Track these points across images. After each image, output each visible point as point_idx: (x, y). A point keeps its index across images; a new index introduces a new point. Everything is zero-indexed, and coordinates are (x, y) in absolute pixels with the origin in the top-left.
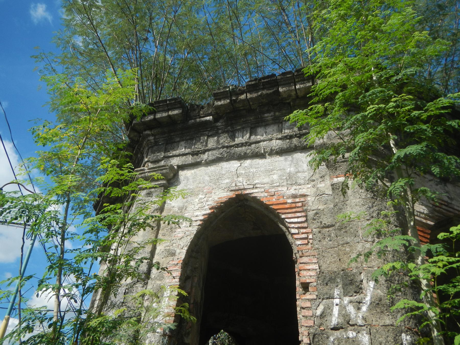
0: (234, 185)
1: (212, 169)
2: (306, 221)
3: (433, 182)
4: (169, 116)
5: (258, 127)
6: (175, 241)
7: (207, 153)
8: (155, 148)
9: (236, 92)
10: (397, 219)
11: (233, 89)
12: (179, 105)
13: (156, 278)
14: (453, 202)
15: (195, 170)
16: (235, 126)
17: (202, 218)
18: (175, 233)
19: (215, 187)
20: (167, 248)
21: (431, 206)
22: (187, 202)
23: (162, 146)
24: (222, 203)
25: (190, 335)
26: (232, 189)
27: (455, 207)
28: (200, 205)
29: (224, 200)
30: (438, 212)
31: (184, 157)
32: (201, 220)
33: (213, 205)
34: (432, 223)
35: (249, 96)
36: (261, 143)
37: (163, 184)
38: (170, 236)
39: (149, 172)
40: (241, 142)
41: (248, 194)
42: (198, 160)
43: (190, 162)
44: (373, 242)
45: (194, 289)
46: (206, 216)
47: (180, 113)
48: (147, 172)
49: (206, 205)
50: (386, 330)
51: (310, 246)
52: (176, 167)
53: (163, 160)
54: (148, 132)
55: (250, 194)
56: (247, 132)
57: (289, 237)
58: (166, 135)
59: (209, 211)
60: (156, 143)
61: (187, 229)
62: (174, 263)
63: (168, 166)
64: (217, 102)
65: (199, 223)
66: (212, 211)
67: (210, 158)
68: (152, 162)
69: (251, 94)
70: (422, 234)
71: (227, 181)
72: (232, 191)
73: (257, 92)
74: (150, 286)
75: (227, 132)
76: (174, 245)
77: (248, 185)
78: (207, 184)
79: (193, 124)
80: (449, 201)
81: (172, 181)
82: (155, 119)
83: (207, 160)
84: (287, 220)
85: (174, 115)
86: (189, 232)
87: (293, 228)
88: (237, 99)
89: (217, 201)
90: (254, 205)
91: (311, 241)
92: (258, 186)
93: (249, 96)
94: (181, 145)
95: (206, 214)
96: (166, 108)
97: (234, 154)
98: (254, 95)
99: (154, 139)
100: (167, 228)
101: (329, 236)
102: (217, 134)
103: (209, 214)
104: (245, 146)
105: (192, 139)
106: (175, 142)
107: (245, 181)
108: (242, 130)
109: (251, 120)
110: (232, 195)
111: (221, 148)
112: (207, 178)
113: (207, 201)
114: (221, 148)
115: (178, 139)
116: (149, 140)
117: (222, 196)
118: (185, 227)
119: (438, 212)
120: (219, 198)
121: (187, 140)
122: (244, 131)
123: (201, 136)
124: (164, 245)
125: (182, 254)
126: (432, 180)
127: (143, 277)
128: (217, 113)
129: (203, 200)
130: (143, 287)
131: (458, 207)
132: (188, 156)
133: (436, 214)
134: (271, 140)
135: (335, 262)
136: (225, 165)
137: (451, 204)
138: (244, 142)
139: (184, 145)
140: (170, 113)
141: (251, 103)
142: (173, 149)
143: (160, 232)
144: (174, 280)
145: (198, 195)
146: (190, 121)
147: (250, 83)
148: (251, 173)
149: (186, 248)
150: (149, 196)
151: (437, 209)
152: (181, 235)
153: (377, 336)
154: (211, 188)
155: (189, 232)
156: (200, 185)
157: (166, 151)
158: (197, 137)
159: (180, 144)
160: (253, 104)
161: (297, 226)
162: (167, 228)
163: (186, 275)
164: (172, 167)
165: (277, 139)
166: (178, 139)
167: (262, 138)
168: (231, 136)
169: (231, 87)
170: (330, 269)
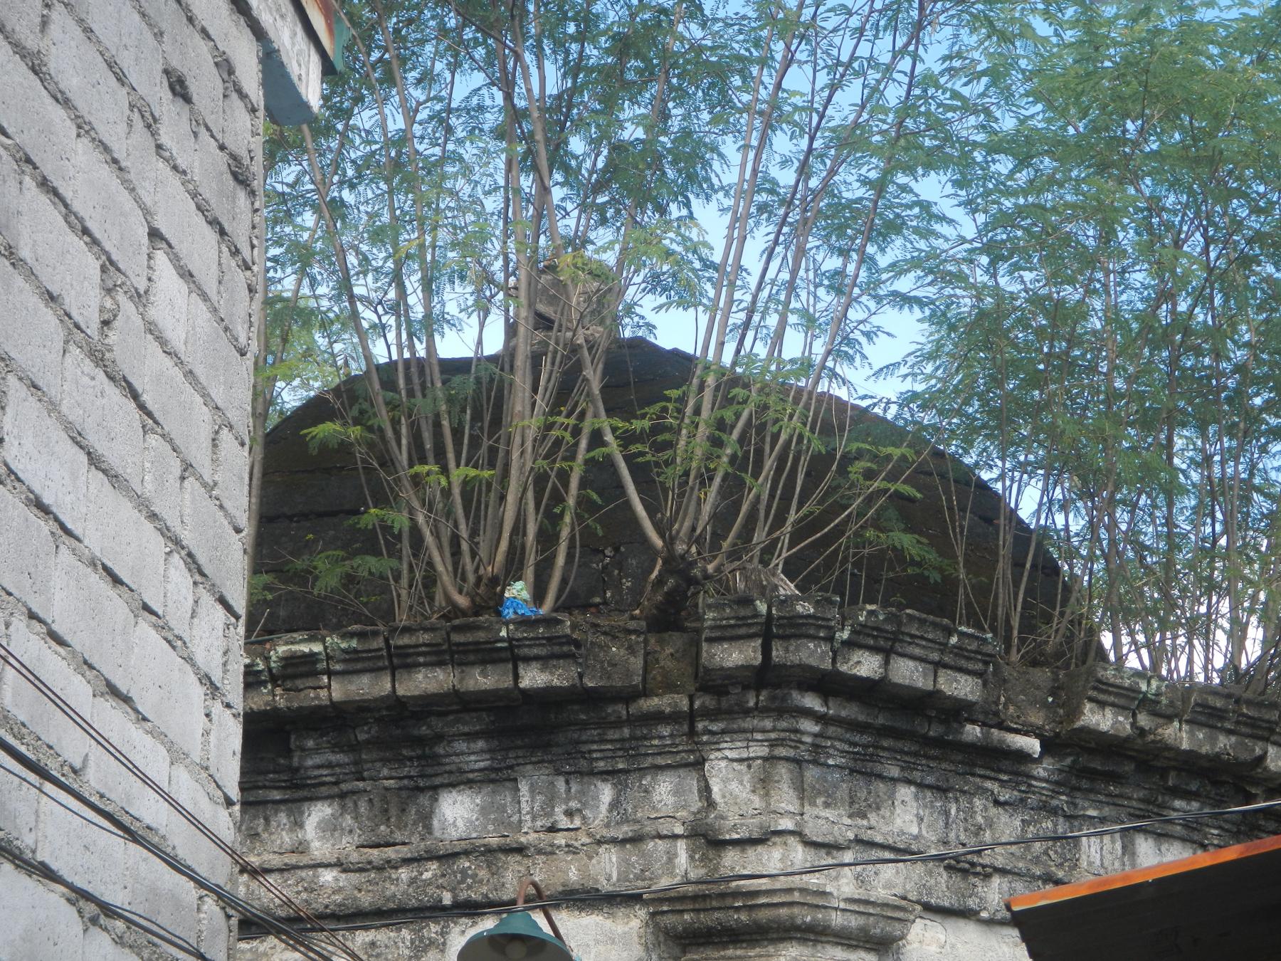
7: (996, 880)
16: (1080, 802)
42: (972, 903)
43: (947, 904)
54: (811, 702)
58: (866, 739)
68: (810, 844)
96: (935, 656)
105: (941, 790)
106: (880, 777)
114: (1039, 878)
115: (895, 772)
116: (796, 731)
121: (921, 786)
123: (974, 795)
139: (913, 807)
146: (969, 727)
166: (895, 772)
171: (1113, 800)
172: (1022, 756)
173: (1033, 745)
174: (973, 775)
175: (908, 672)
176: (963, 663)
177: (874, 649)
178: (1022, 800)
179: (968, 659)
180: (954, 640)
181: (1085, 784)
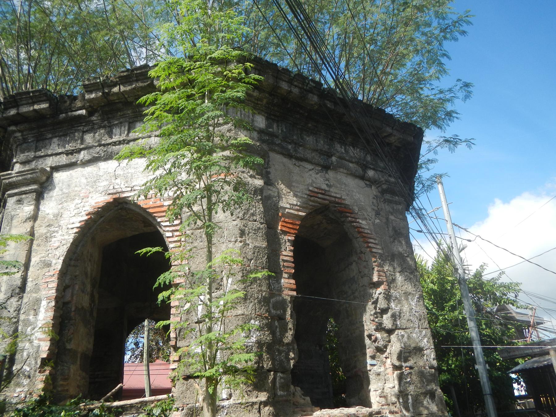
0: (111, 187)
1: (90, 170)
2: (181, 222)
3: (313, 171)
4: (35, 110)
5: (137, 121)
6: (50, 251)
7: (82, 152)
8: (24, 146)
9: (108, 84)
10: (264, 216)
11: (104, 80)
12: (45, 98)
13: (31, 291)
14: (331, 190)
15: (71, 172)
16: (112, 121)
17: (79, 225)
18: (51, 243)
19: (92, 190)
20: (42, 259)
21: (306, 196)
22: (62, 208)
23: (32, 144)
24: (99, 208)
25: (73, 341)
26: (110, 192)
27: (333, 194)
28: (77, 210)
29: (101, 205)
30: (313, 201)
31: (58, 156)
32: (77, 228)
33: (90, 211)
34: (304, 214)
35: (123, 88)
36: (140, 141)
37: (35, 189)
38: (45, 246)
39: (17, 176)
40: (119, 139)
41: (125, 197)
42: (73, 161)
43: (65, 163)
44: (236, 242)
45: (75, 296)
46: (83, 223)
47: (47, 108)
48: (14, 177)
49: (83, 211)
50: (237, 319)
51: (181, 249)
52: (48, 169)
53: (34, 160)
54: (13, 128)
55: (128, 197)
56: (125, 127)
57: (166, 239)
59: (86, 218)
60: (25, 141)
61: (63, 238)
62: (50, 274)
63: (38, 169)
64: (88, 94)
65: (76, 230)
66: (89, 217)
67: (88, 157)
69: (124, 87)
70: (291, 226)
71: (105, 183)
72: (109, 194)
73: (132, 85)
74: (25, 300)
75: (104, 127)
76: (50, 255)
77: (126, 187)
78: (84, 187)
79: (64, 118)
80: (327, 189)
81: (46, 185)
82: (18, 114)
83: (83, 161)
84: (162, 223)
85: (40, 109)
86: (65, 241)
87: (168, 231)
88: (110, 91)
89: (94, 206)
90: (133, 208)
91: (183, 243)
92: (135, 188)
93: (123, 88)
94: (54, 142)
95: (83, 221)
96: (30, 101)
97: (111, 152)
98: (128, 88)
99: (22, 135)
100: (42, 238)
101: (201, 237)
102: (92, 130)
103: (86, 221)
104: (123, 144)
105: (65, 135)
106: (46, 139)
107: (123, 183)
108: (120, 125)
109: (128, 114)
110: (109, 199)
111: (97, 146)
112: (84, 181)
113: (84, 207)
114: (97, 146)
115: (50, 136)
116: (16, 137)
117: (99, 201)
118: (61, 235)
119: (313, 201)
120: (96, 203)
121: (60, 136)
122: (121, 126)
124: (39, 256)
125: (58, 264)
126: (313, 169)
127: (17, 291)
128: (90, 106)
129: (79, 206)
130: (18, 301)
131: (336, 193)
132: (62, 156)
133: (311, 203)
134: (150, 137)
135: (203, 262)
136: (102, 165)
137: (329, 191)
138: (121, 139)
140: (36, 107)
141: (126, 96)
142: (45, 147)
143: (34, 242)
144: (51, 292)
145: (74, 200)
146: (61, 115)
147: (122, 74)
148: (130, 174)
149: (62, 258)
150: (20, 204)
151: (312, 198)
152: (57, 244)
153: (230, 325)
154: (88, 192)
155: (65, 241)
156: (76, 189)
157: (37, 149)
158: (72, 133)
159: (53, 141)
160: (129, 97)
161: (171, 229)
162: (42, 238)
163: (64, 285)
164: (43, 170)
165: (155, 136)
166: (50, 136)
167: (140, 135)
168: (108, 132)
169: (101, 78)
170: (198, 269)
171: (122, 116)
172: (80, 116)
173: (83, 112)
174: (74, 127)
175: (25, 109)
176: (40, 99)
177: (13, 107)
178: (92, 128)
179: (40, 97)
180: (31, 94)
181: (110, 116)
